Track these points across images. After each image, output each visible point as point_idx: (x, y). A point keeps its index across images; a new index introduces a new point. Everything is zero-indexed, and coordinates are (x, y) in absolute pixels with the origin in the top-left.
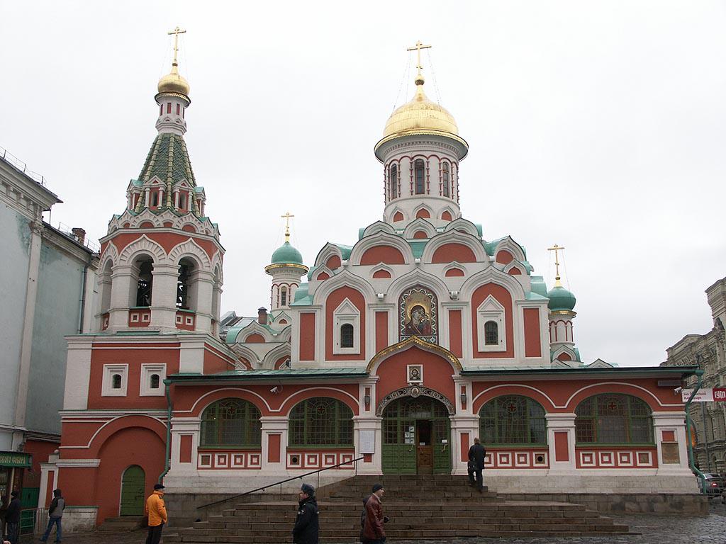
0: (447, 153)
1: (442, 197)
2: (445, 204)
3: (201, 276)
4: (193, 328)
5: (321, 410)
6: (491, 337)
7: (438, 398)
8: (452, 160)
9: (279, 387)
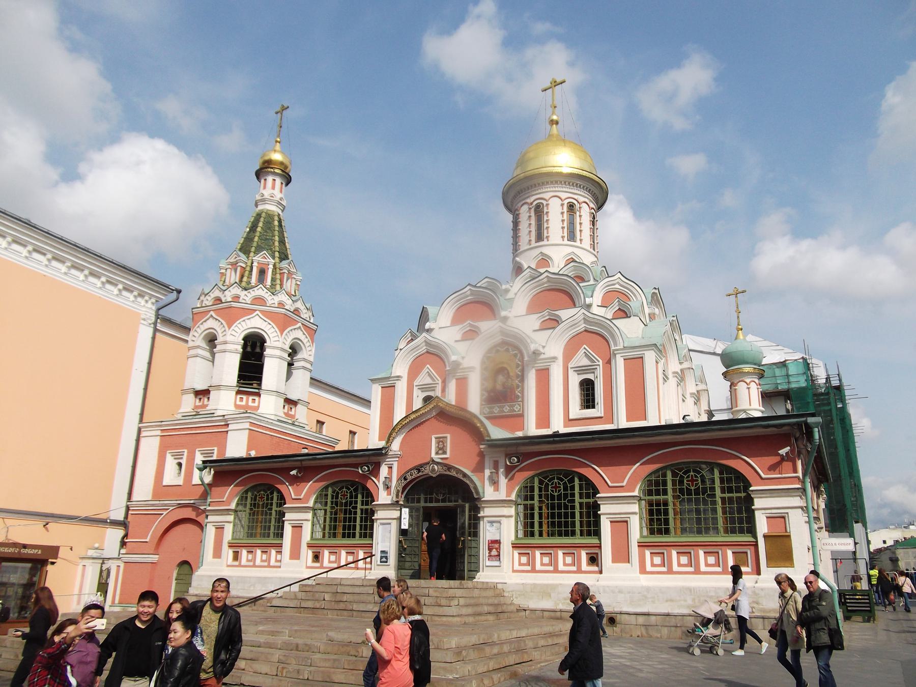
0: (571, 191)
1: (566, 242)
2: (570, 250)
3: (267, 352)
4: (257, 408)
5: (344, 495)
6: (588, 401)
7: (460, 477)
8: (581, 199)
9: (300, 469)
